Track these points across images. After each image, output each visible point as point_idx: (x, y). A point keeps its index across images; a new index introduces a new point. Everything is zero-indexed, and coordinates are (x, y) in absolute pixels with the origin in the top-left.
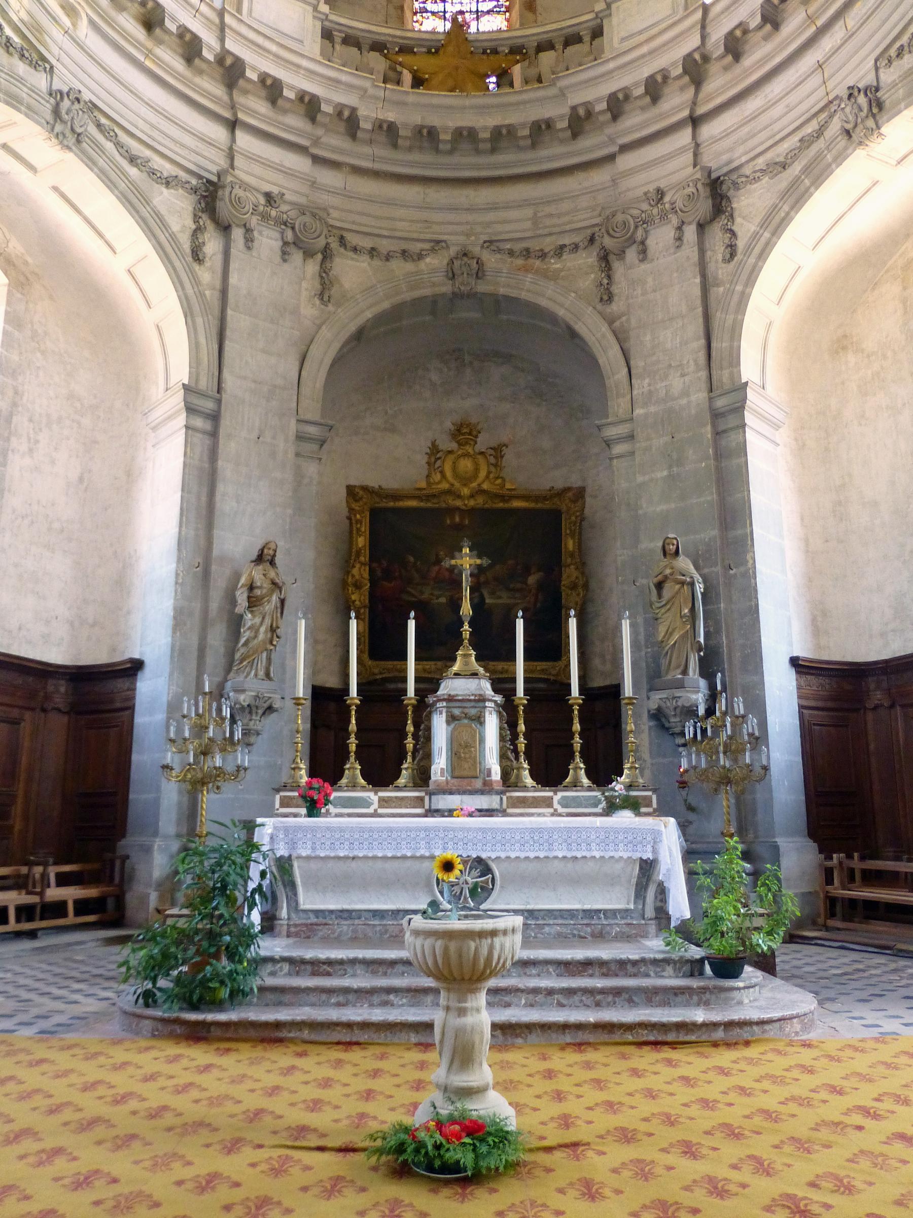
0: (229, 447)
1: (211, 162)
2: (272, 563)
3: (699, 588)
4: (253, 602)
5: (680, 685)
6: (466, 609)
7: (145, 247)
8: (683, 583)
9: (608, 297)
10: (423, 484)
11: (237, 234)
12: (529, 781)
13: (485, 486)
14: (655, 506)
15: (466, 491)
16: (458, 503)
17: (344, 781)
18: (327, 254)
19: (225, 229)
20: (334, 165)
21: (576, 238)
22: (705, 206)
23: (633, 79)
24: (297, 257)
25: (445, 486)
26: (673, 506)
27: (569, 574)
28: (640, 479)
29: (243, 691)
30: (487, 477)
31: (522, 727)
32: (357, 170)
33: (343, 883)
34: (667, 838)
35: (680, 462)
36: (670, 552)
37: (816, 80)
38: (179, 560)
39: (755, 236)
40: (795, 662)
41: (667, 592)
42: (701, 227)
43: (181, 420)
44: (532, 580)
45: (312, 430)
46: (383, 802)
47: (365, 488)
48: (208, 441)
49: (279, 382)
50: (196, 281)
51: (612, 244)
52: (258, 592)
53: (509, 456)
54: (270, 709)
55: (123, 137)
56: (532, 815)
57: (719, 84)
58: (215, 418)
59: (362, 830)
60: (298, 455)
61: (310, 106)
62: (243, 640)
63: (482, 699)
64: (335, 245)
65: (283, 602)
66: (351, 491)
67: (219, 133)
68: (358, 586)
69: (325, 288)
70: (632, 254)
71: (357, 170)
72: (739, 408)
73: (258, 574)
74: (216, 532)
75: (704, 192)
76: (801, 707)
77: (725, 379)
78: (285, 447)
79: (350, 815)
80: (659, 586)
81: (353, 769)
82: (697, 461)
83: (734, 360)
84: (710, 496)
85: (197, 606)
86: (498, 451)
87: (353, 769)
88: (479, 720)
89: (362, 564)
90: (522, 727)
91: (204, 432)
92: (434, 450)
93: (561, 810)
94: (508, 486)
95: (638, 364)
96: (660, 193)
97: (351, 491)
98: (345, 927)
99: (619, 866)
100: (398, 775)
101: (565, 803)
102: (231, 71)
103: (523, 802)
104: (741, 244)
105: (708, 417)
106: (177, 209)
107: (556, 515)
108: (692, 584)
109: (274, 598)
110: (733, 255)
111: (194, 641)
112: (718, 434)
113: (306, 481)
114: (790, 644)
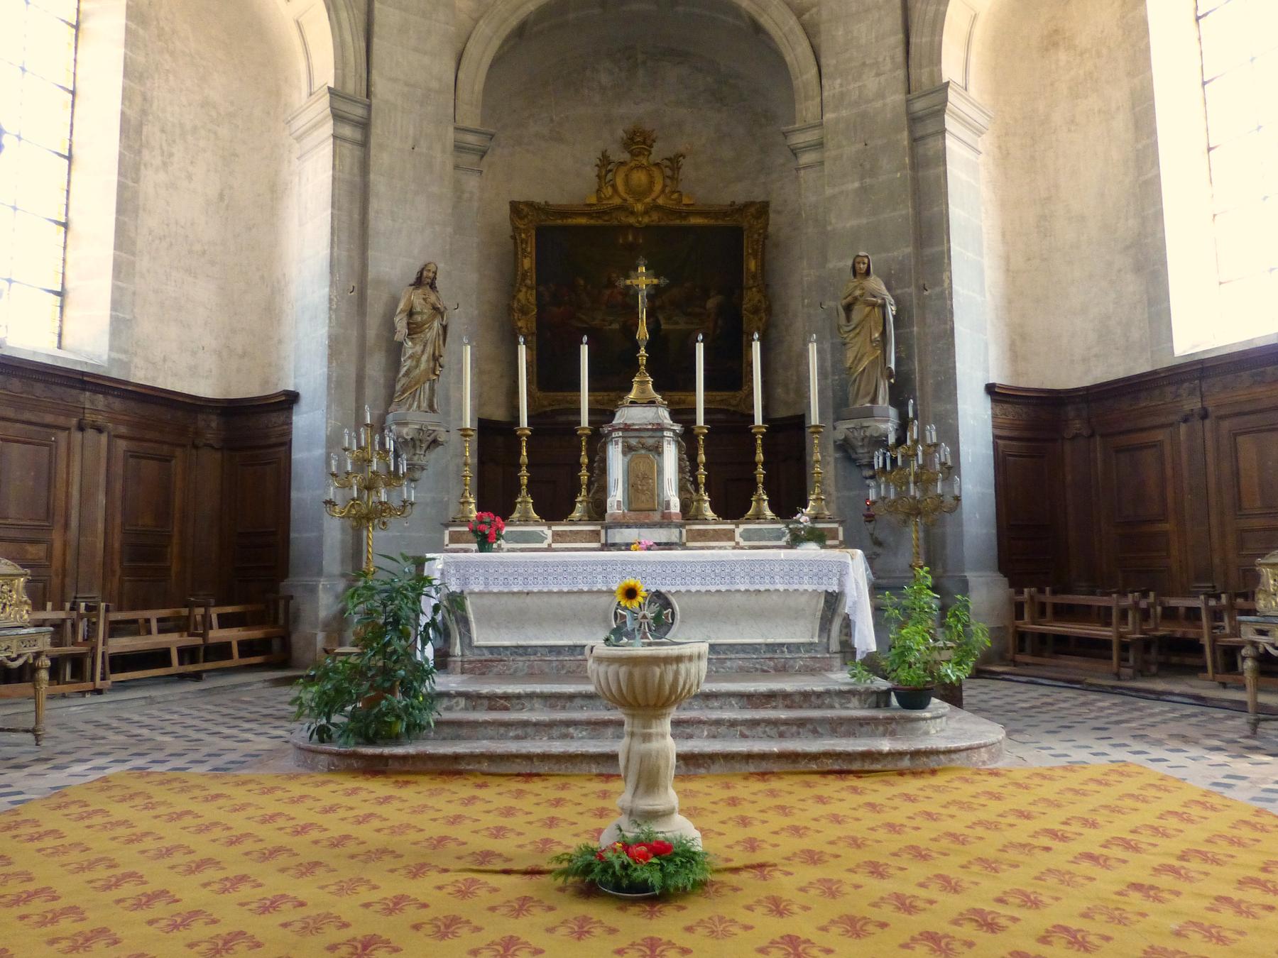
0: (381, 159)
2: (432, 286)
3: (891, 310)
4: (414, 329)
5: (869, 414)
6: (643, 333)
8: (874, 305)
10: (593, 200)
12: (709, 514)
13: (660, 201)
14: (844, 221)
15: (639, 207)
16: (632, 220)
17: (516, 515)
25: (617, 201)
26: (864, 221)
27: (751, 297)
28: (829, 191)
29: (406, 424)
30: (663, 191)
31: (702, 458)
33: (518, 618)
34: (853, 571)
36: (860, 272)
38: (332, 284)
40: (991, 389)
41: (857, 315)
44: (711, 304)
45: (471, 138)
46: (558, 536)
47: (530, 205)
48: (358, 152)
49: (434, 85)
52: (418, 318)
53: (687, 166)
54: (435, 443)
56: (713, 548)
58: (364, 125)
59: (536, 564)
60: (456, 167)
62: (404, 370)
63: (660, 428)
65: (445, 328)
66: (515, 208)
68: (524, 311)
72: (938, 112)
73: (417, 299)
74: (371, 253)
76: (996, 437)
77: (925, 79)
78: (443, 158)
79: (522, 550)
80: (848, 308)
81: (525, 503)
82: (892, 170)
84: (906, 210)
85: (354, 334)
86: (674, 162)
87: (525, 503)
88: (658, 450)
89: (529, 288)
90: (702, 458)
91: (353, 142)
92: (604, 161)
93: (742, 543)
94: (685, 201)
95: (829, 62)
97: (515, 208)
98: (521, 663)
99: (803, 599)
100: (572, 509)
101: (748, 536)
103: (703, 535)
105: (904, 120)
107: (737, 233)
108: (883, 306)
109: (436, 324)
111: (352, 371)
112: (915, 140)
113: (466, 196)
114: (987, 370)
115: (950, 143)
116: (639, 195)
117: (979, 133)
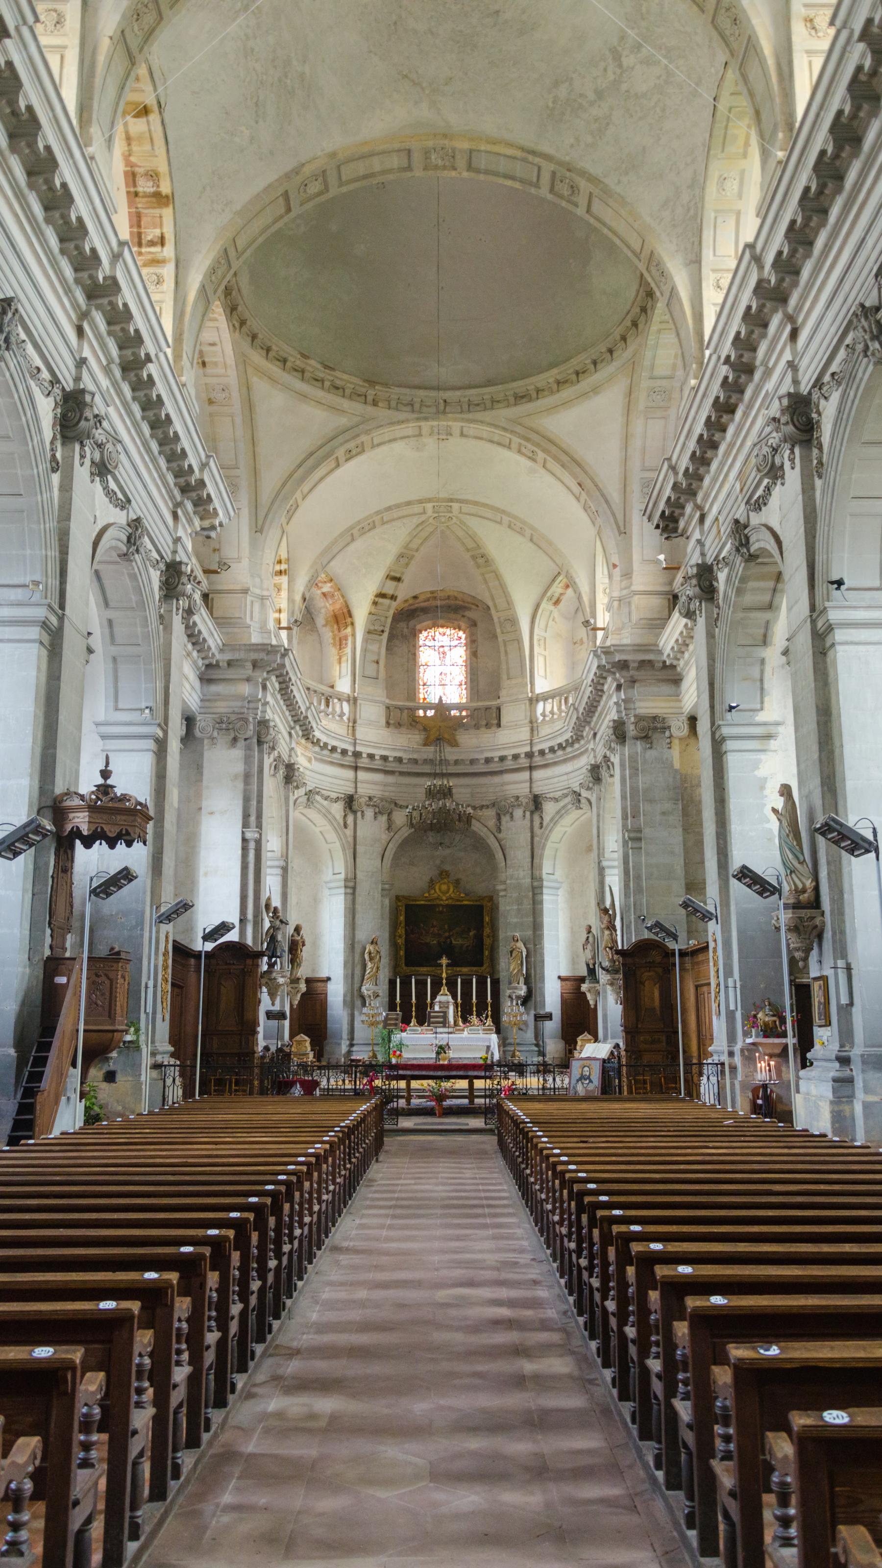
0: (359, 899)
1: (351, 791)
4: (371, 959)
5: (516, 988)
6: (444, 975)
7: (329, 827)
9: (499, 830)
11: (359, 814)
18: (389, 814)
19: (355, 812)
20: (392, 773)
21: (488, 803)
22: (533, 808)
23: (509, 753)
24: (379, 817)
27: (487, 931)
32: (402, 773)
35: (521, 904)
37: (565, 777)
39: (548, 825)
40: (559, 977)
42: (532, 813)
43: (342, 890)
44: (471, 934)
45: (387, 886)
50: (345, 834)
51: (502, 809)
55: (324, 792)
57: (538, 761)
58: (354, 888)
61: (385, 758)
64: (393, 806)
66: (398, 898)
67: (350, 774)
68: (400, 937)
69: (389, 828)
70: (508, 817)
71: (402, 773)
75: (531, 803)
78: (377, 895)
80: (511, 952)
82: (527, 905)
83: (541, 869)
92: (432, 880)
95: (508, 862)
96: (518, 797)
102: (357, 755)
104: (545, 824)
106: (337, 809)
107: (480, 908)
110: (541, 827)
112: (534, 894)
115: (545, 897)
116: (444, 893)
117: (558, 888)
